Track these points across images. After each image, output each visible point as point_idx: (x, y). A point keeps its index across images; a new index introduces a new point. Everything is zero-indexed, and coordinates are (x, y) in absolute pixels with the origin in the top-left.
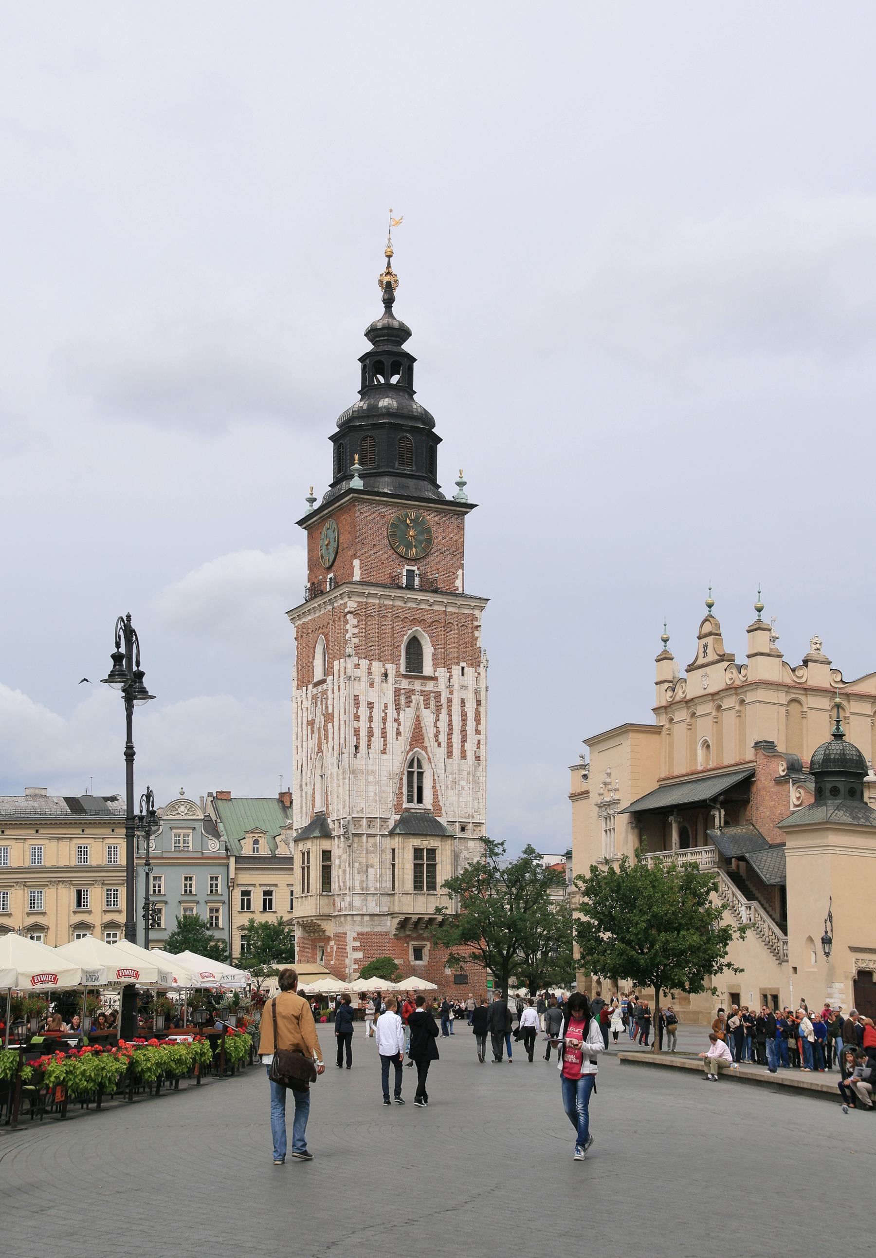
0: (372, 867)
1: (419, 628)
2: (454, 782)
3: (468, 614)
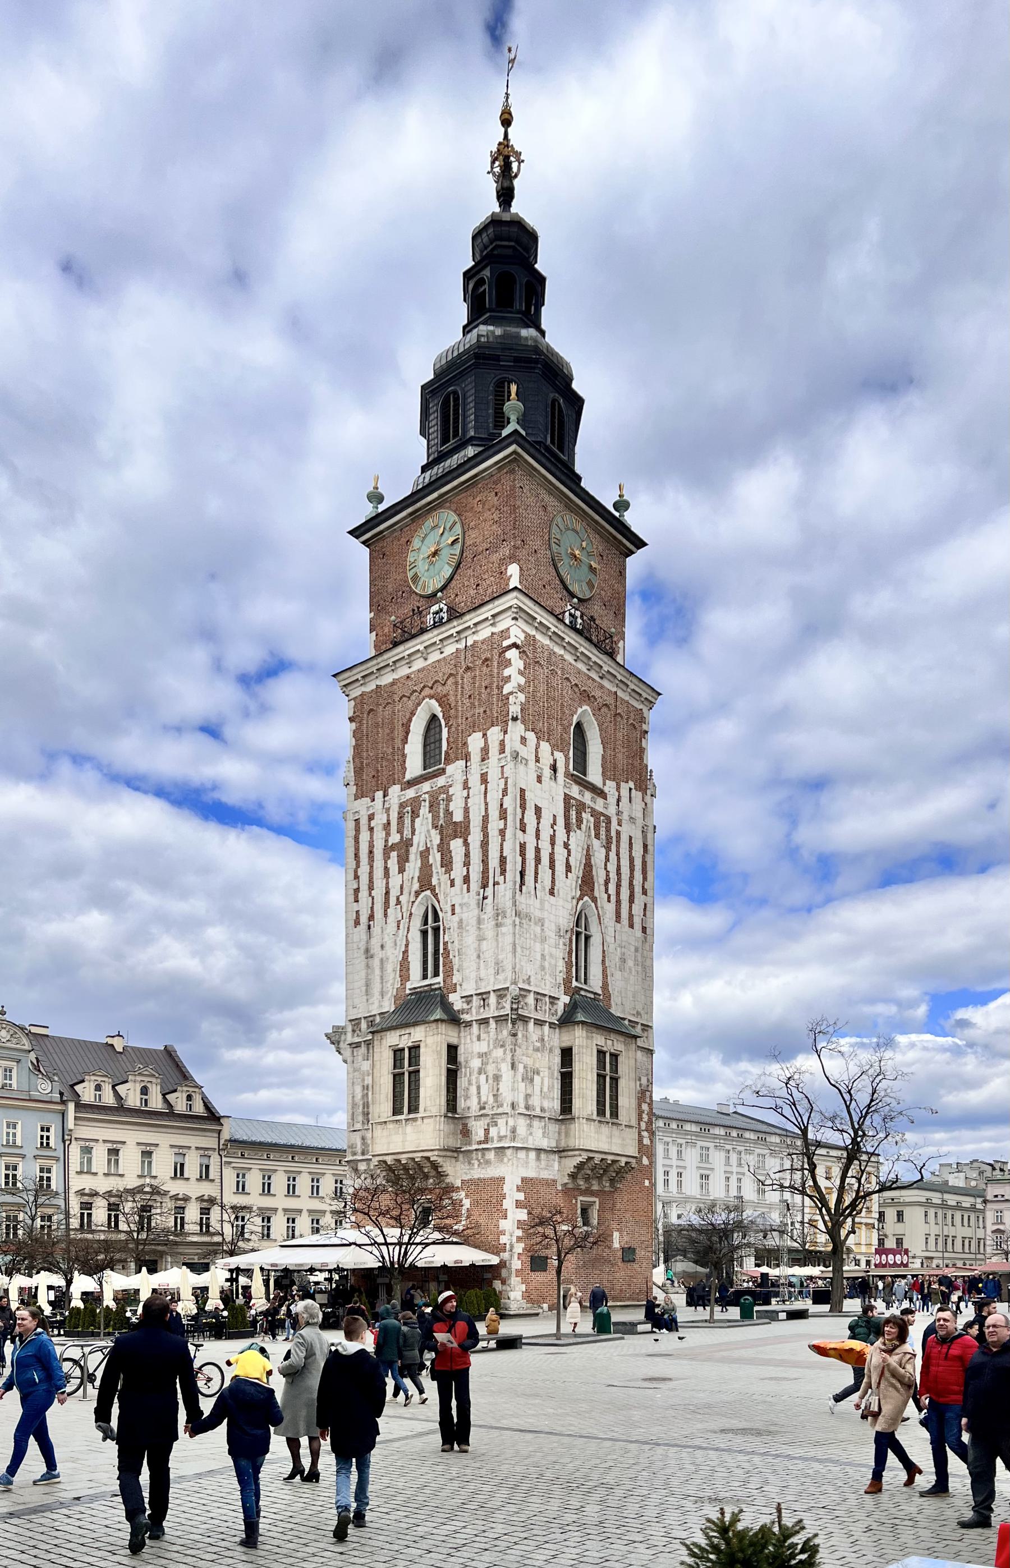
0: (538, 1074)
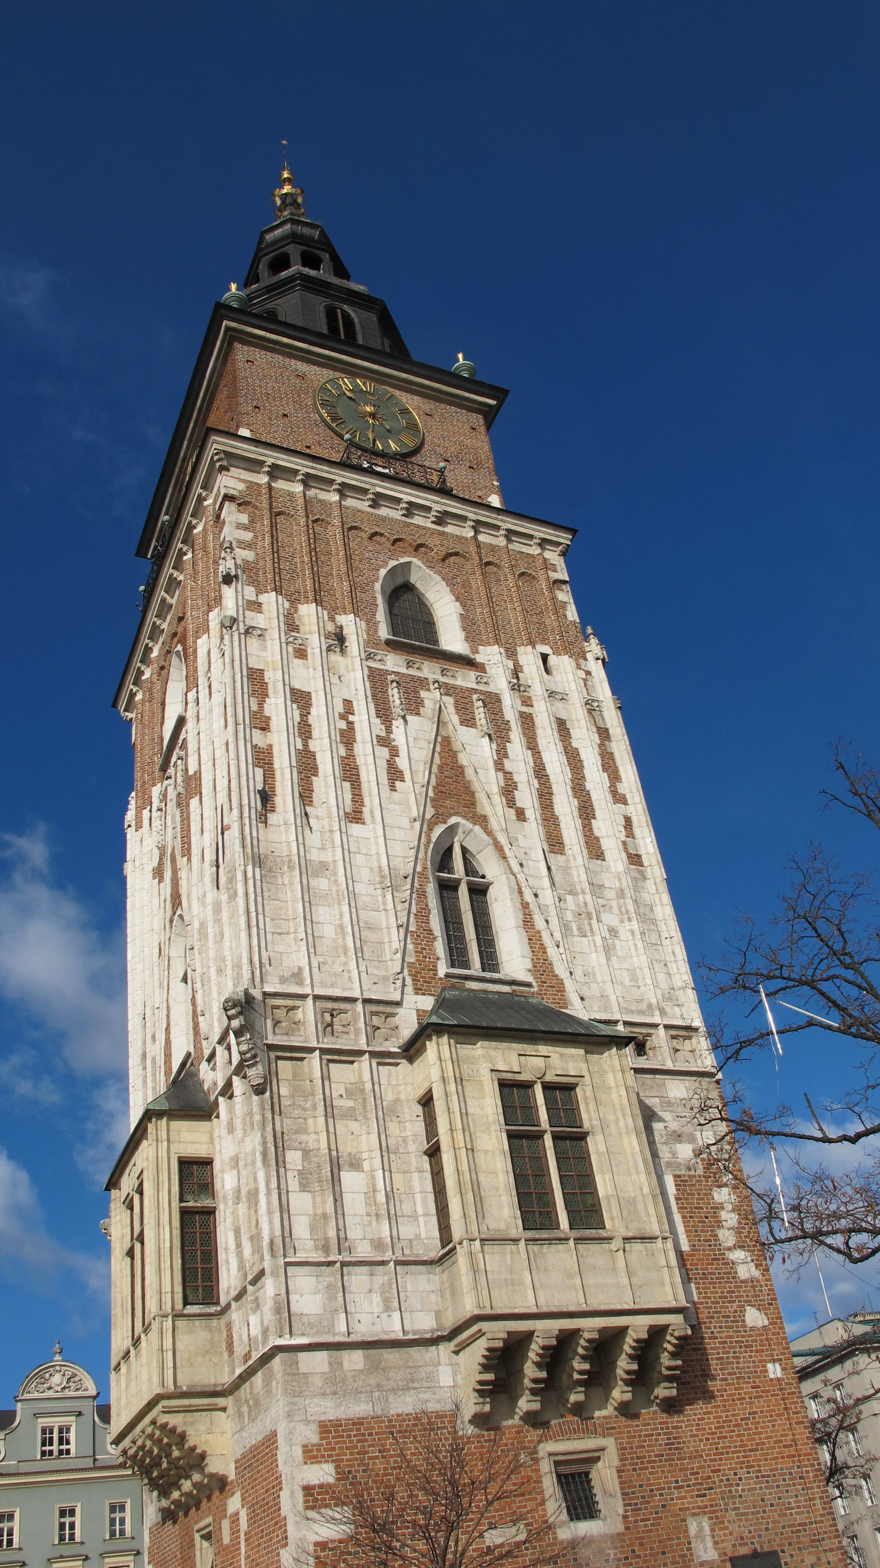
0: (355, 1165)
3: (533, 556)
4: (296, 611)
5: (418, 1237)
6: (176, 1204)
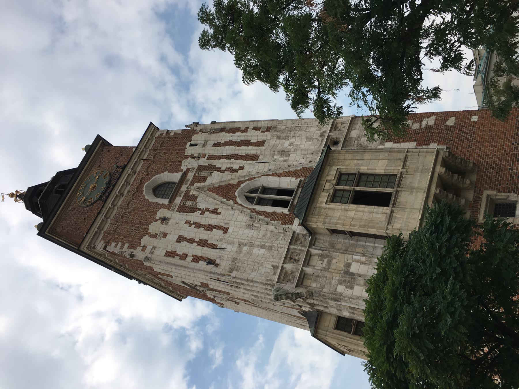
0: (348, 265)
1: (146, 184)
2: (283, 153)
4: (150, 233)
5: (382, 248)
6: (351, 336)
